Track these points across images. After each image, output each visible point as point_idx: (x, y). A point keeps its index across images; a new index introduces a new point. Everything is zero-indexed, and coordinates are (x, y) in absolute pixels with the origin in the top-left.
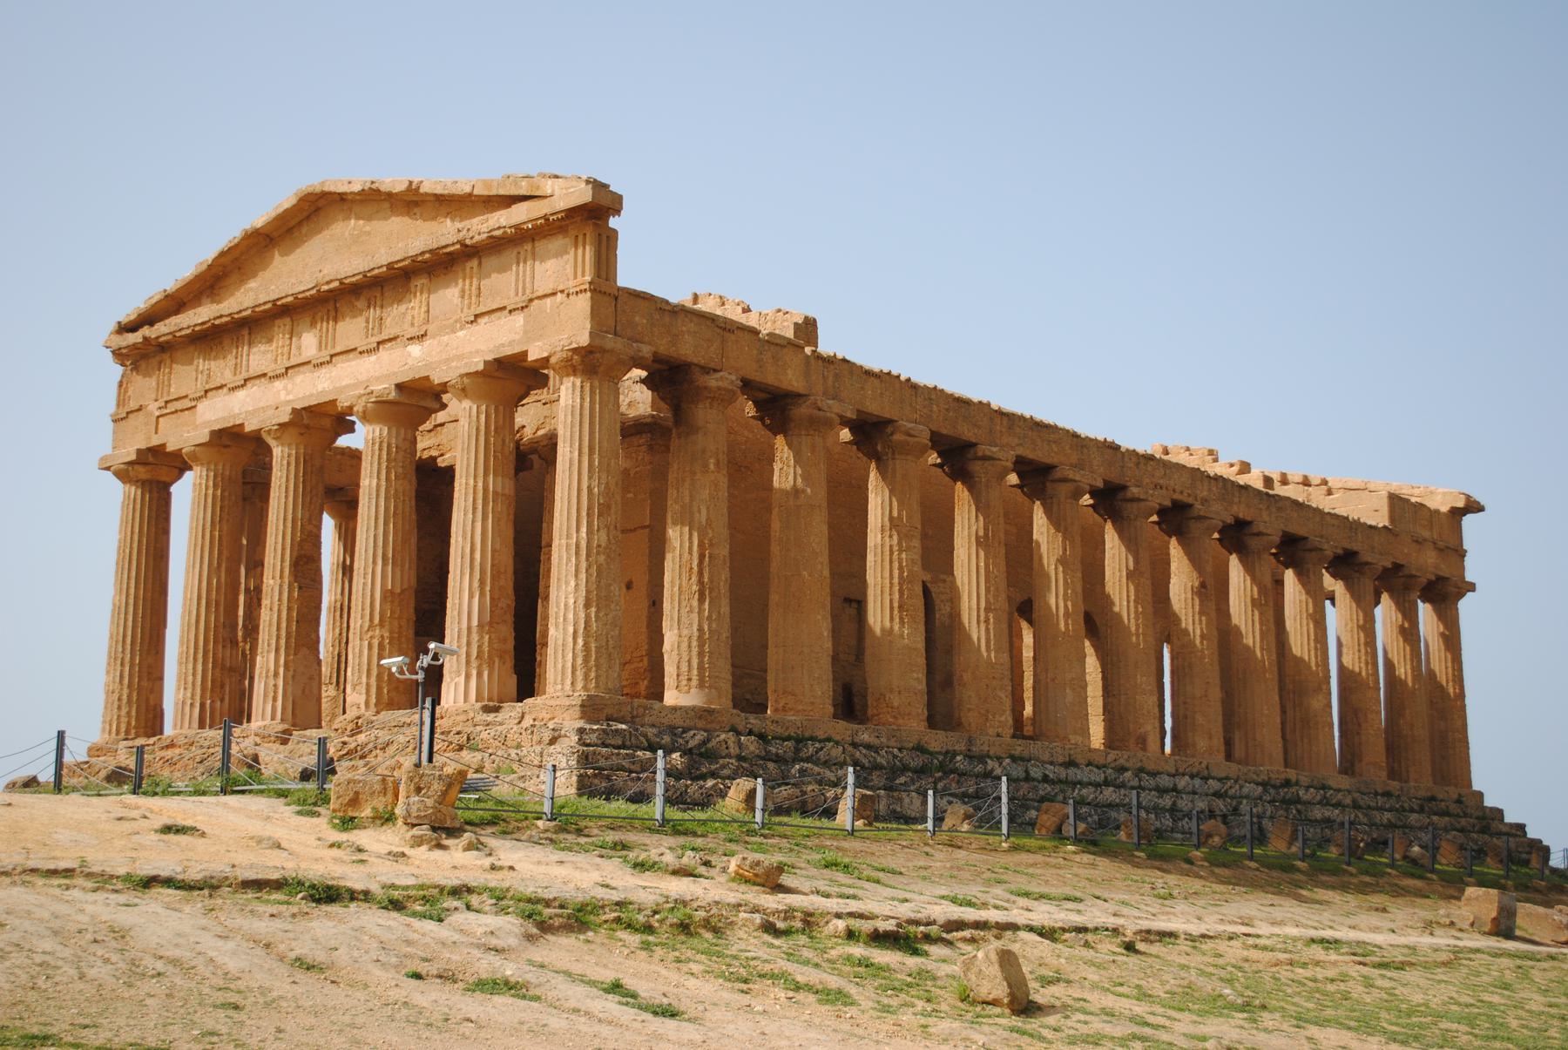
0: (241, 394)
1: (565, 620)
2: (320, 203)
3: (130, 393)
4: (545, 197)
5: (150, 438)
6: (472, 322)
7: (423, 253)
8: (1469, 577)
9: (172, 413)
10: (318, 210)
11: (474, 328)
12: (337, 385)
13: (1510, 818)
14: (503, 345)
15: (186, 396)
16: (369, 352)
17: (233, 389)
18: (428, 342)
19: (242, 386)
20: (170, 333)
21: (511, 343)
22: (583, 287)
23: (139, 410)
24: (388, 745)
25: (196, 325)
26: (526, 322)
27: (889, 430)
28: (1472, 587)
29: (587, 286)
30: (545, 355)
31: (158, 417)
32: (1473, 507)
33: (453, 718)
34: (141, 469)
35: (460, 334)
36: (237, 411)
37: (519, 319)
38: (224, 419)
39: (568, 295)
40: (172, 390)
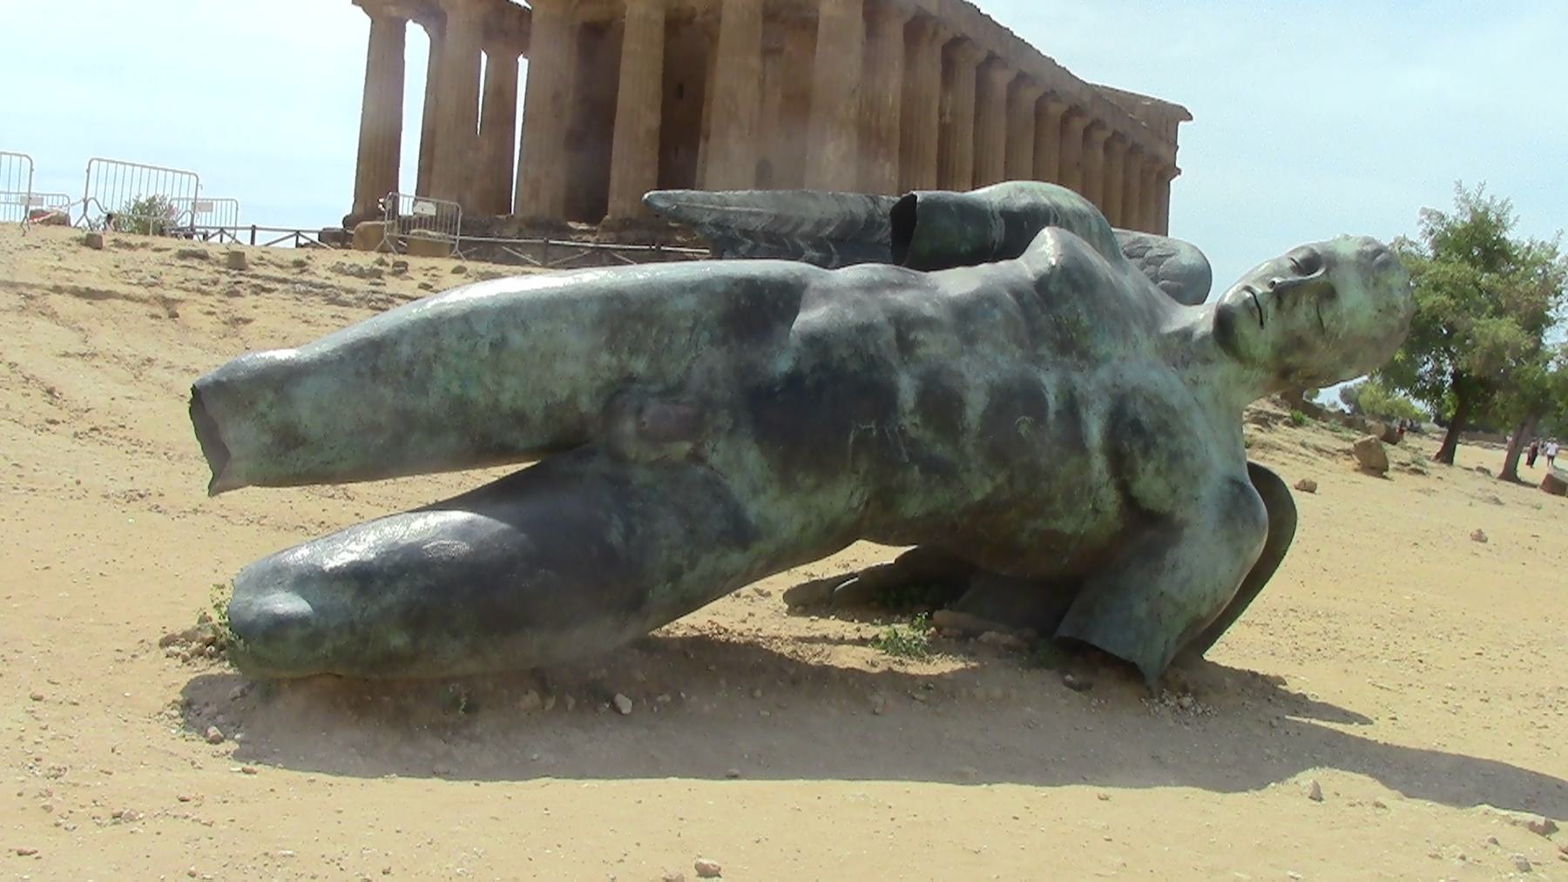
8: (1178, 165)
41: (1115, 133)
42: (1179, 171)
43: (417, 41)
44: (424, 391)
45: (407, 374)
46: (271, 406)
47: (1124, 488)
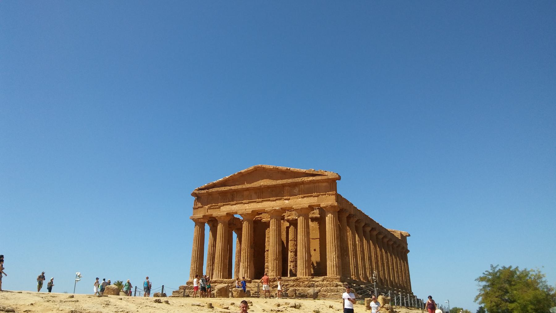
1: (333, 260)
2: (257, 169)
5: (205, 213)
14: (312, 203)
16: (273, 201)
24: (288, 285)
32: (409, 235)
33: (303, 280)
34: (202, 220)
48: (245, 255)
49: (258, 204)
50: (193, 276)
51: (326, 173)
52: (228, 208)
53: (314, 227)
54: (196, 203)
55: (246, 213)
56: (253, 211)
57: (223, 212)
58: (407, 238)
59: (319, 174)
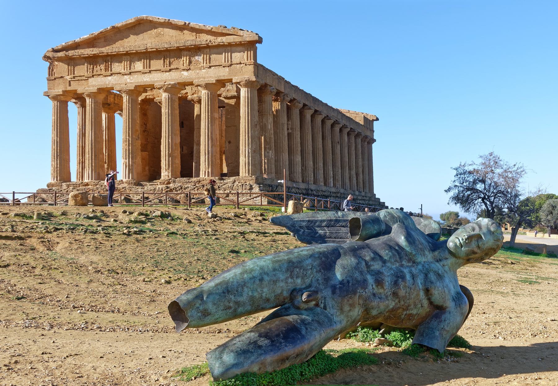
0: (109, 78)
2: (141, 22)
3: (55, 70)
4: (241, 36)
6: (208, 68)
7: (192, 45)
8: (375, 138)
9: (77, 80)
10: (140, 24)
11: (210, 70)
12: (153, 80)
13: (381, 201)
15: (84, 76)
16: (166, 71)
17: (105, 76)
18: (190, 72)
19: (110, 76)
20: (79, 55)
21: (224, 76)
22: (251, 63)
23: (62, 77)
24: (186, 188)
25: (91, 54)
26: (230, 71)
27: (295, 102)
28: (375, 141)
29: (253, 63)
30: (239, 81)
31: (69, 81)
32: (377, 119)
34: (62, 97)
35: (203, 71)
36: (107, 83)
37: (227, 69)
38: (102, 85)
39: (246, 65)
40: (75, 73)
41: (351, 128)
42: (375, 141)
43: (73, 108)
44: (242, 295)
45: (237, 291)
46: (200, 305)
47: (429, 299)
48: (127, 148)
49: (143, 75)
50: (55, 176)
51: (241, 33)
52: (100, 80)
53: (229, 110)
54: (51, 72)
55: (127, 89)
56: (136, 86)
57: (93, 86)
58: (375, 122)
59: (231, 33)
